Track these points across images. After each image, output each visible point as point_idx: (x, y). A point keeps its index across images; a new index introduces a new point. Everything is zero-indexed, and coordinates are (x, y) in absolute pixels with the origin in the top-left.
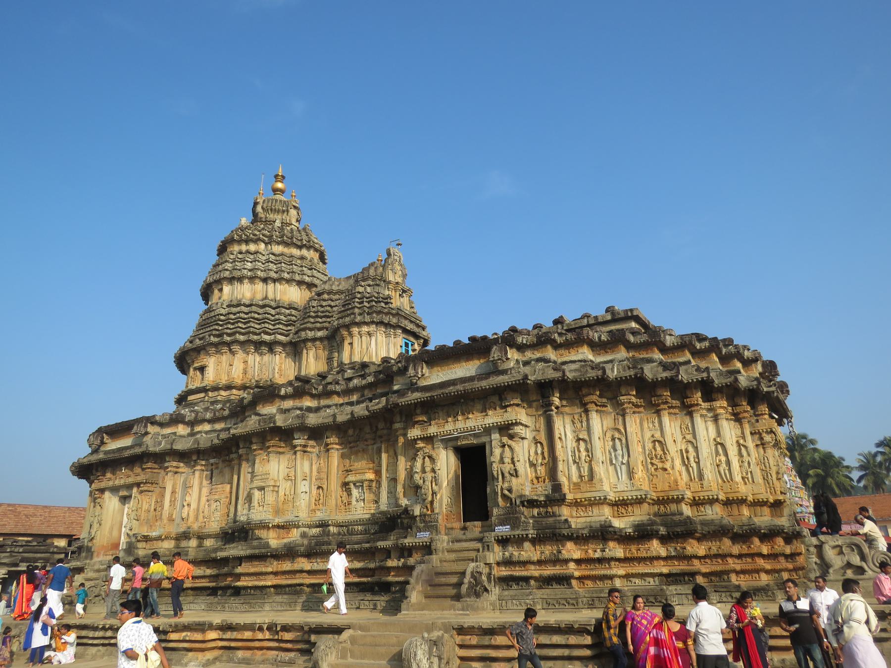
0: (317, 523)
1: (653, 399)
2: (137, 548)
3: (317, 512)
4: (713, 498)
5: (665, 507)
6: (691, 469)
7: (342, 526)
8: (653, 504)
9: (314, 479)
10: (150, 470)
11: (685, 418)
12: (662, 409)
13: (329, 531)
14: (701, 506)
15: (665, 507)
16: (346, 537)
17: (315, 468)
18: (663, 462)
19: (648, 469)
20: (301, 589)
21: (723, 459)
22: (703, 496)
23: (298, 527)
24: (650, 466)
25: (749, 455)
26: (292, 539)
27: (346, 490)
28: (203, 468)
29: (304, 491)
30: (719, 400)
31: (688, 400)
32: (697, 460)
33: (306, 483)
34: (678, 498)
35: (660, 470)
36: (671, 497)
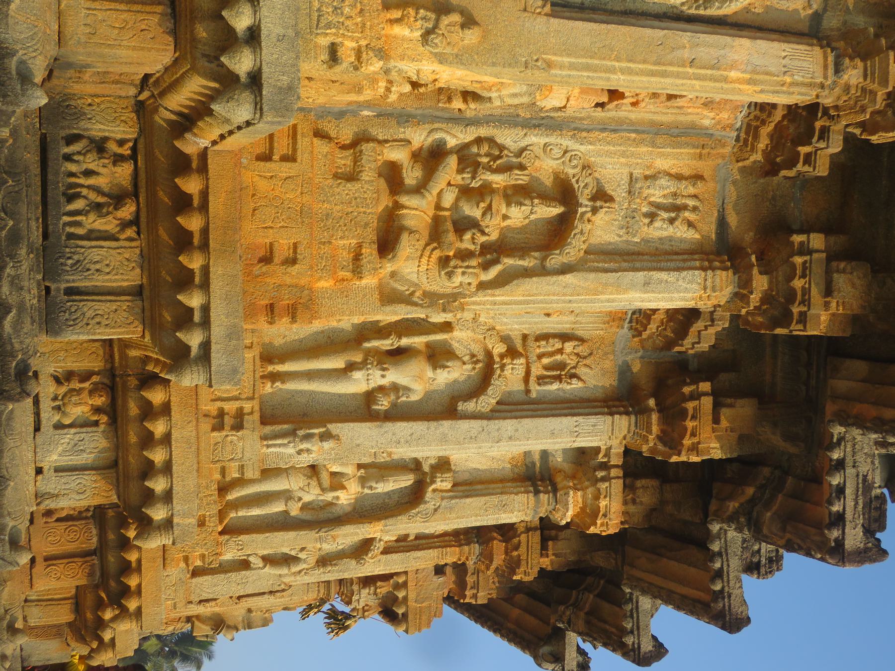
1: (817, 241)
4: (149, 497)
5: (118, 199)
6: (337, 363)
8: (140, 108)
11: (608, 364)
12: (745, 284)
14: (100, 401)
15: (118, 199)
18: (436, 234)
19: (404, 118)
21: (345, 498)
22: (167, 439)
24: (420, 137)
25: (324, 561)
30: (625, 503)
31: (707, 402)
32: (383, 404)
34: (185, 318)
35: (385, 201)
36: (195, 263)
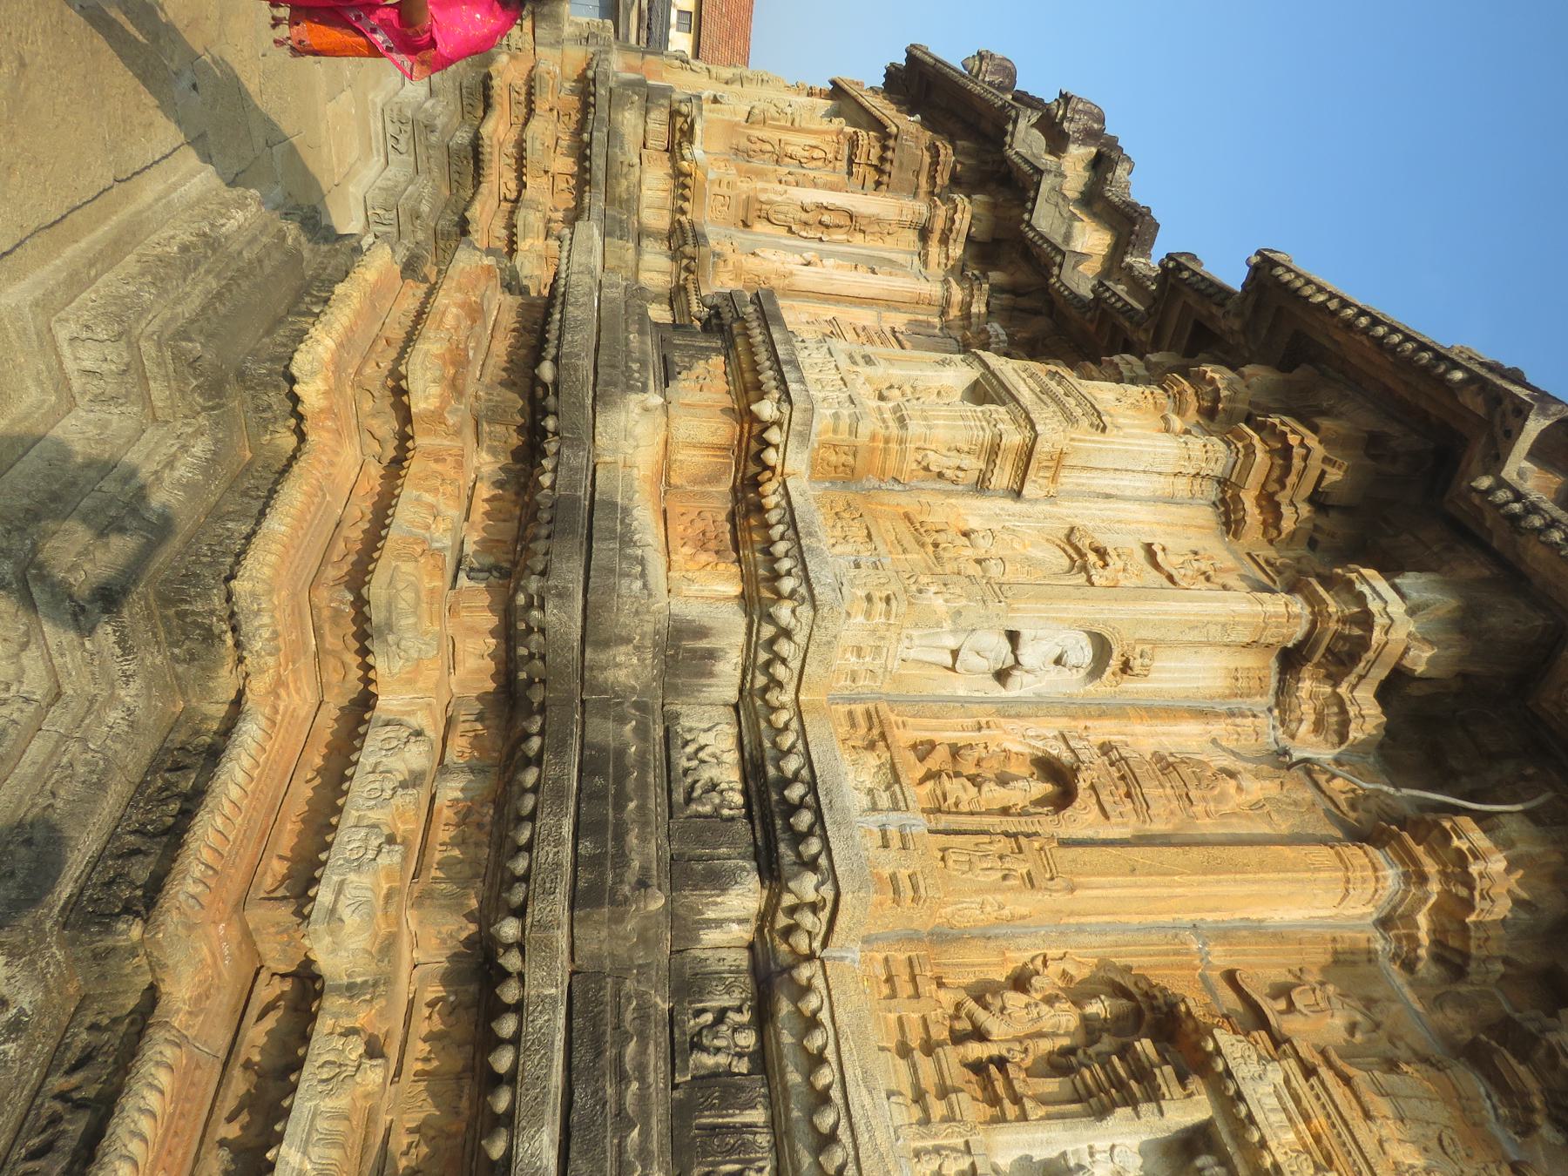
0: (792, 764)
2: (647, 113)
3: (872, 760)
7: (763, 1017)
9: (1104, 730)
10: (927, 159)
13: (719, 880)
16: (657, 1076)
17: (1186, 737)
20: (210, 637)
23: (756, 604)
26: (656, 564)
27: (1091, 1029)
28: (954, 312)
29: (1027, 655)
33: (1070, 683)
